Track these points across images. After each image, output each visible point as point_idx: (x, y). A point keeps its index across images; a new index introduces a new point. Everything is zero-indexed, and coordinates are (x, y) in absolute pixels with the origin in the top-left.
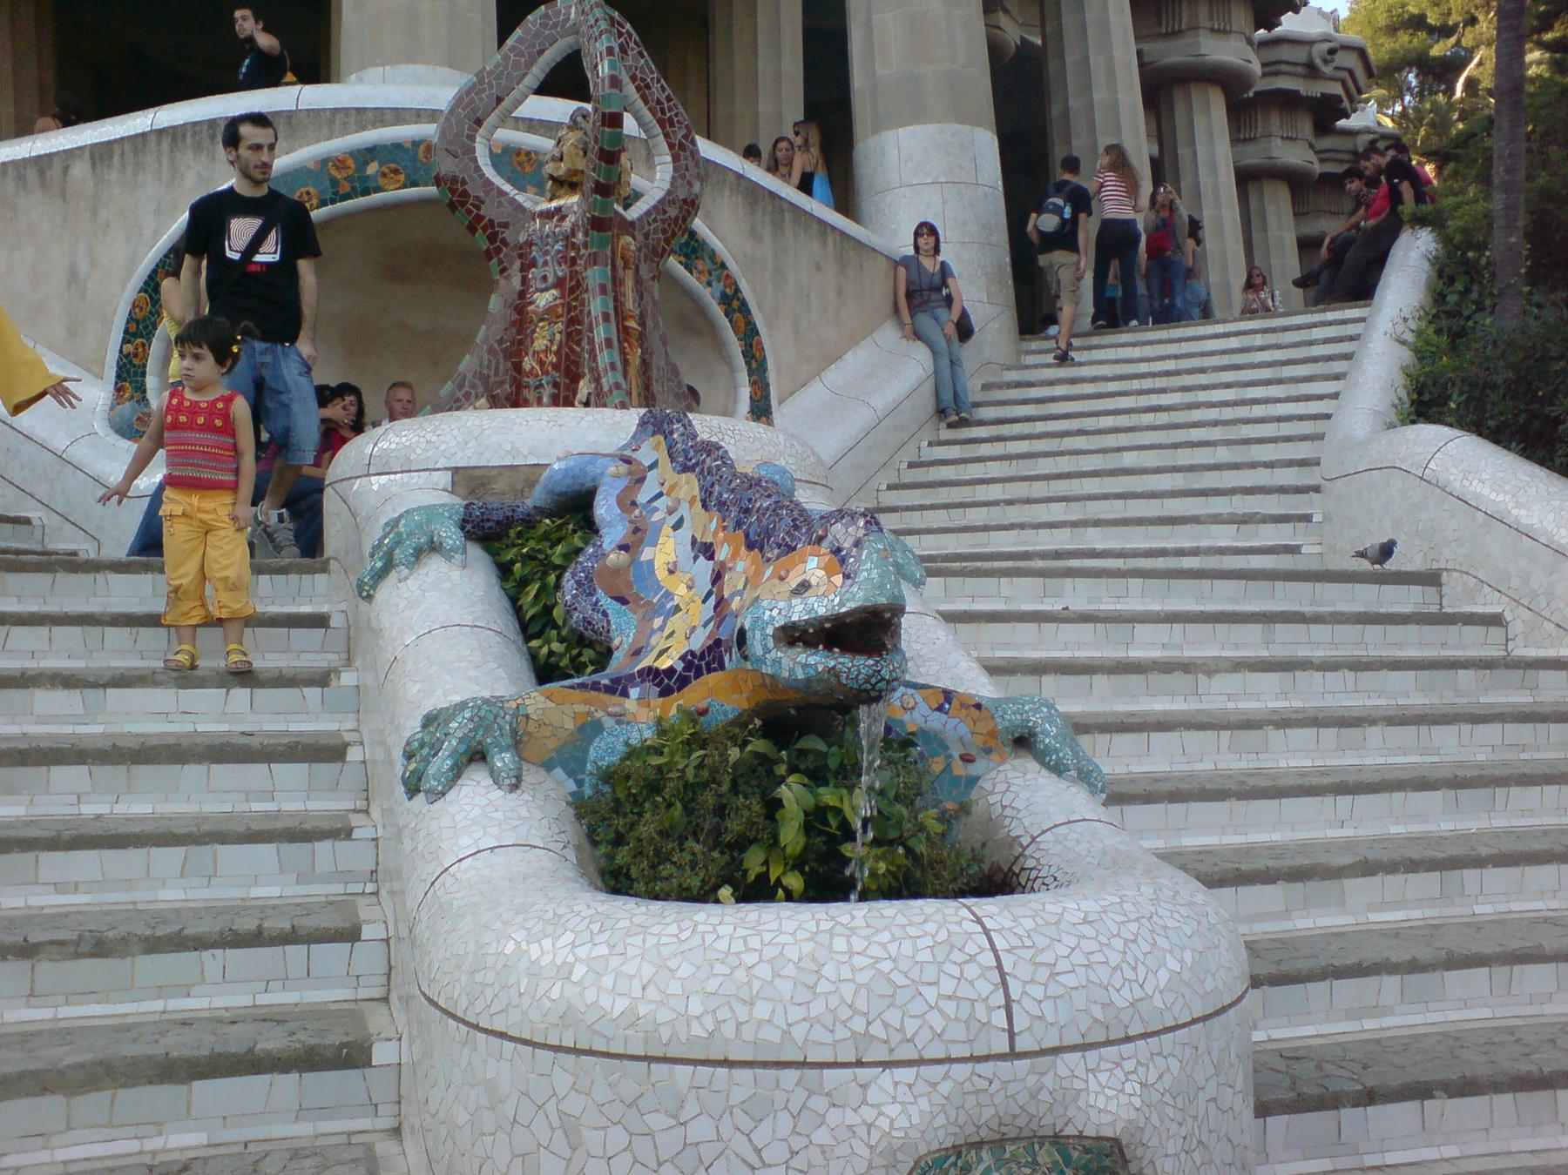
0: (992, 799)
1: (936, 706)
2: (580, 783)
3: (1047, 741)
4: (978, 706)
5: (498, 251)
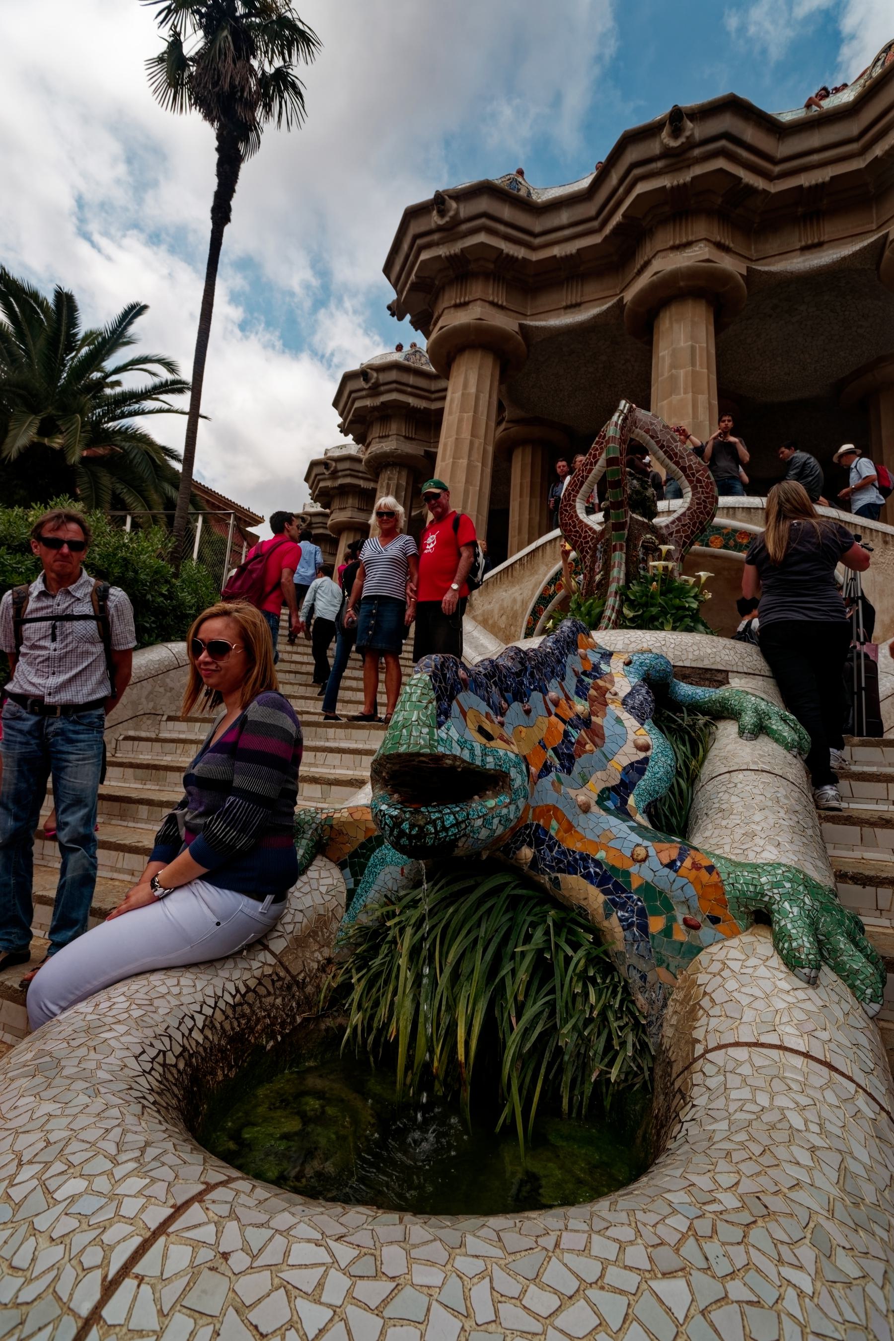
0: (702, 978)
1: (666, 861)
2: (357, 883)
3: (783, 923)
4: (711, 869)
5: (585, 557)
